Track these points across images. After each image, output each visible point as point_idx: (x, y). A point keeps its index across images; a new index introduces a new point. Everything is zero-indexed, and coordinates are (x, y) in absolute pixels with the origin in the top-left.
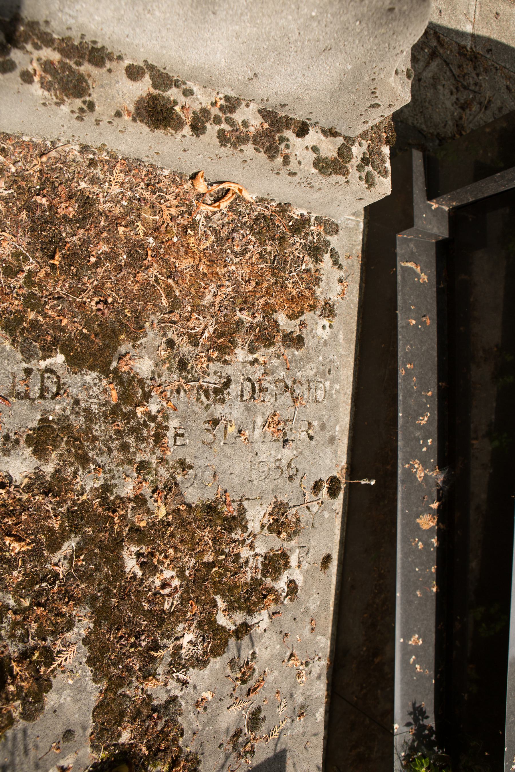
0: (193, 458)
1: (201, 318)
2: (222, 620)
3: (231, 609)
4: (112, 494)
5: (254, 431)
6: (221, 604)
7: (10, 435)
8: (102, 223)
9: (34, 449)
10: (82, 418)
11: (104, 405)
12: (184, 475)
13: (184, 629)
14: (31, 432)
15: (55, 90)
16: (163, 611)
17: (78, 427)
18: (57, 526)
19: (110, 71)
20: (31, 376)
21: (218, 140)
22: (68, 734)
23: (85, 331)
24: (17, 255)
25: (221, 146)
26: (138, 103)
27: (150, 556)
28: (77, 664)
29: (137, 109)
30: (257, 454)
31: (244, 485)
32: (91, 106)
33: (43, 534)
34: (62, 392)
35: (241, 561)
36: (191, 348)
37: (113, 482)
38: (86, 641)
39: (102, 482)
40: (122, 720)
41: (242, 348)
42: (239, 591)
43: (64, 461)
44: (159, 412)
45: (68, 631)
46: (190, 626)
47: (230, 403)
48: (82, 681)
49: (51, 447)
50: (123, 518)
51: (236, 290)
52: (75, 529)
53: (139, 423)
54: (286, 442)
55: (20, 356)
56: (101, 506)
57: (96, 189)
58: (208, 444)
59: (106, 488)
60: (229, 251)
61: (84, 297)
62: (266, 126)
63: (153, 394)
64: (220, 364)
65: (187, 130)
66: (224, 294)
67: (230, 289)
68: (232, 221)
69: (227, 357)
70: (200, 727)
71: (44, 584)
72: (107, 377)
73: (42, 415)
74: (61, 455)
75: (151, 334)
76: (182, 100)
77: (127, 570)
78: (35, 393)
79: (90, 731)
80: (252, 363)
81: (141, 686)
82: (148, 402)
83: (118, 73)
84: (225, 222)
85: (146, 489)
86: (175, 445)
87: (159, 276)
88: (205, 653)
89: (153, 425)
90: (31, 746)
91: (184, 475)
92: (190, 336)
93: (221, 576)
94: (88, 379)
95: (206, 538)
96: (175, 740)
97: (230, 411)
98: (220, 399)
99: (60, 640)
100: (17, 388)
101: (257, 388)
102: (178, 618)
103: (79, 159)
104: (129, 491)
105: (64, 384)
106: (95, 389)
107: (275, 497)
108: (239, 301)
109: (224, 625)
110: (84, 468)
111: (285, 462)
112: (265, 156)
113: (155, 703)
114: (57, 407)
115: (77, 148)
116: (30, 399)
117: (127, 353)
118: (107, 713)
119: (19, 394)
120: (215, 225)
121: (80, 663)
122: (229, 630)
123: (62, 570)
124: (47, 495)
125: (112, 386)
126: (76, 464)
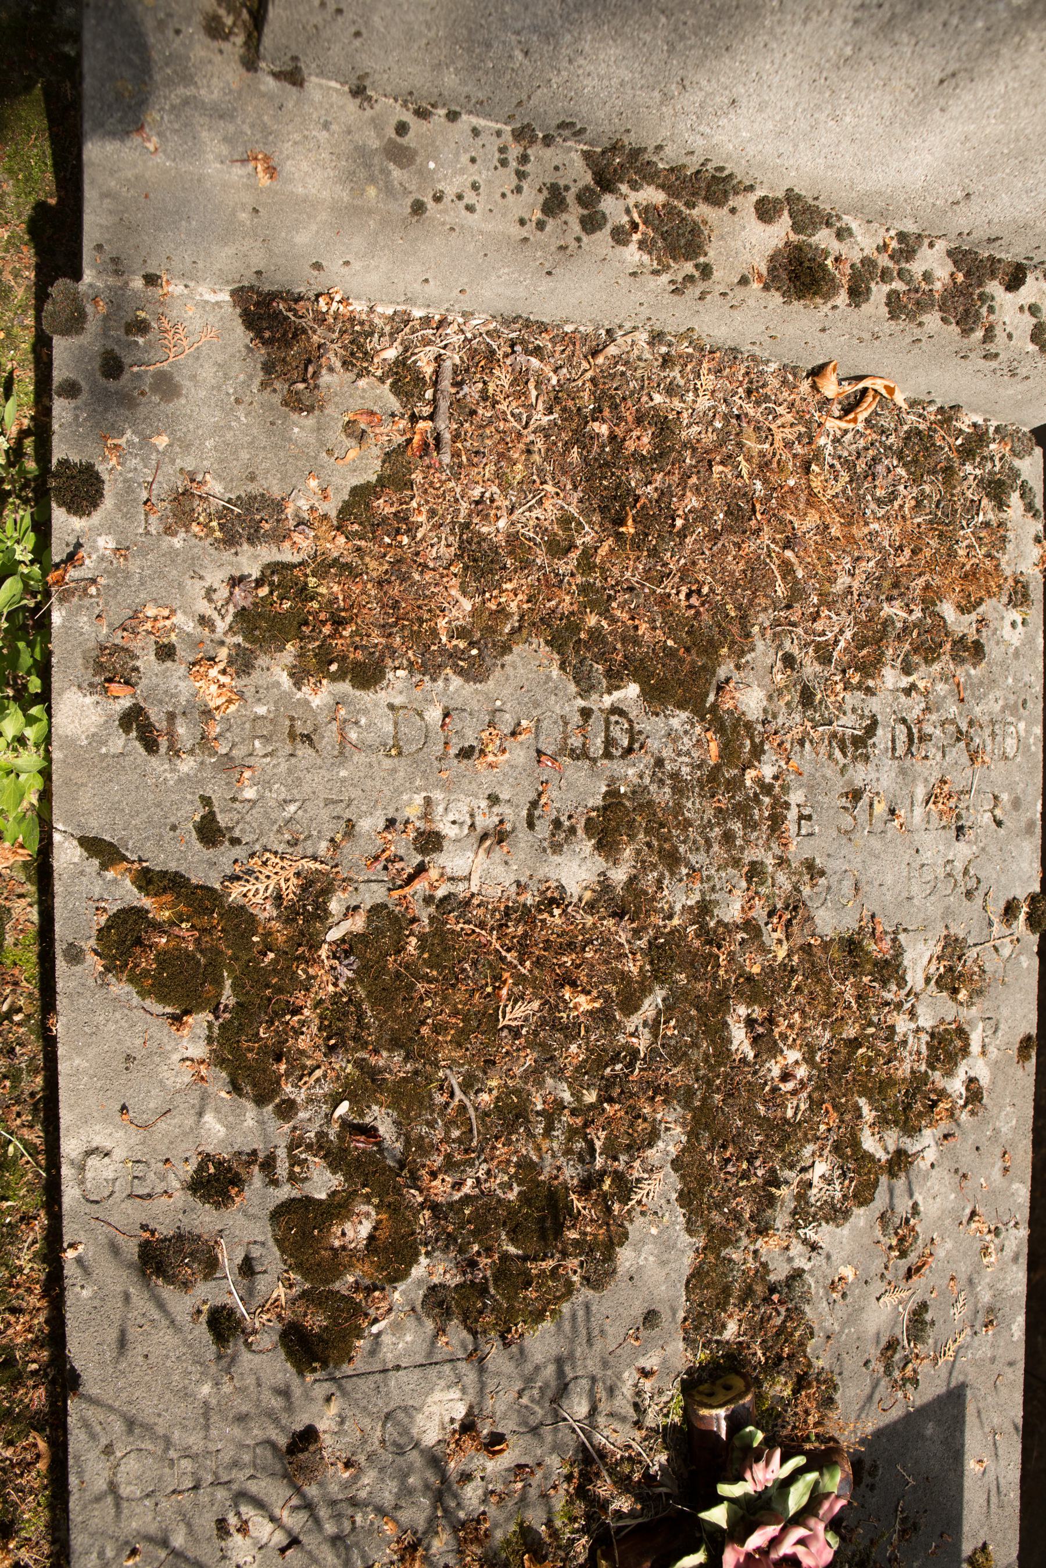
0: (825, 858)
1: (833, 616)
2: (869, 1143)
3: (882, 1122)
4: (712, 917)
5: (912, 811)
6: (868, 1114)
7: (562, 819)
8: (688, 461)
9: (599, 842)
10: (667, 790)
11: (699, 767)
12: (813, 886)
13: (813, 1154)
14: (594, 814)
15: (659, 250)
16: (786, 1121)
17: (663, 805)
18: (635, 971)
19: (733, 211)
20: (591, 721)
21: (887, 309)
22: (651, 1317)
23: (670, 643)
24: (565, 521)
25: (891, 318)
26: (772, 259)
27: (767, 1024)
28: (663, 1201)
29: (771, 270)
30: (917, 851)
31: (900, 905)
32: (706, 271)
33: (614, 983)
34: (636, 746)
35: (897, 1038)
36: (818, 668)
37: (713, 897)
38: (677, 1164)
39: (696, 897)
40: (726, 1303)
41: (893, 666)
42: (895, 1091)
43: (643, 862)
44: (776, 778)
45: (650, 1145)
46: (822, 1149)
47: (876, 761)
48: (671, 1231)
49: (625, 838)
50: (731, 957)
51: (881, 564)
52: (659, 976)
53: (748, 798)
54: (960, 829)
55: (573, 688)
56: (698, 936)
57: (677, 404)
58: (846, 832)
59: (704, 908)
60: (869, 497)
61: (667, 587)
62: (960, 277)
63: (766, 747)
64: (860, 694)
65: (842, 298)
66: (864, 572)
67: (872, 564)
68: (872, 444)
69: (871, 683)
70: (837, 1328)
71: (618, 1067)
72: (703, 719)
73: (608, 786)
74: (638, 852)
75: (760, 645)
76: (835, 246)
77: (733, 1048)
78: (597, 749)
79: (681, 1314)
80: (908, 691)
81: (752, 1248)
82: (759, 761)
83: (744, 213)
84: (860, 447)
85: (759, 913)
86: (798, 835)
87: (772, 546)
88: (845, 1197)
89: (767, 800)
91: (813, 886)
92: (818, 647)
93: (870, 1062)
94: (675, 723)
95: (847, 996)
96: (802, 1344)
97: (877, 775)
98: (861, 754)
99: (638, 1161)
100: (569, 741)
101: (916, 735)
102: (806, 1134)
103: (647, 355)
104: (736, 914)
105: (640, 732)
106: (685, 740)
107: (947, 927)
108: (886, 584)
109: (871, 1150)
110: (672, 874)
111: (959, 866)
112: (958, 330)
113: (772, 1278)
114: (631, 772)
115: (645, 336)
116: (589, 759)
117: (728, 680)
118: (707, 1287)
119: (573, 750)
120: (846, 454)
121: (668, 1202)
122: (879, 1160)
123: (642, 1043)
124: (622, 918)
125: (709, 735)
126: (661, 867)
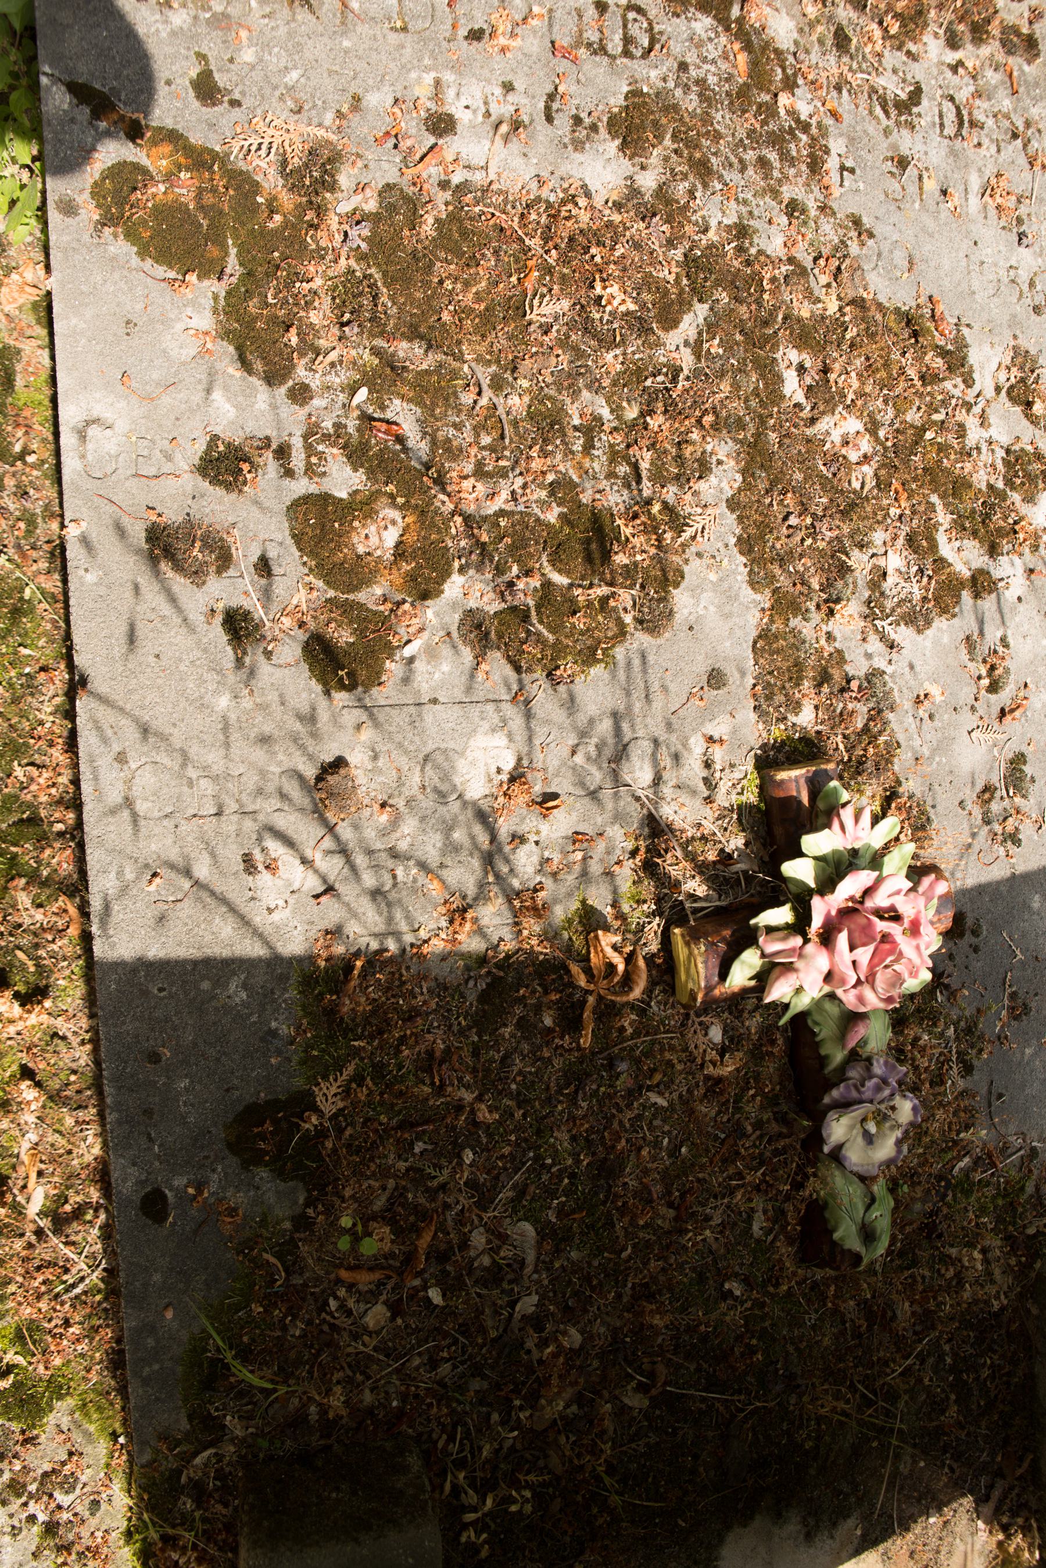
5: (967, 200)
6: (943, 518)
22: (715, 678)
28: (720, 545)
30: (975, 243)
54: (1021, 236)
72: (728, 29)
74: (666, 159)
78: (616, 46)
80: (954, 68)
81: (824, 628)
90: (655, 686)
101: (966, 118)
105: (661, 33)
106: (710, 47)
107: (1015, 337)
110: (705, 186)
111: (1024, 277)
114: (654, 74)
121: (727, 546)
123: (686, 360)
126: (691, 178)
